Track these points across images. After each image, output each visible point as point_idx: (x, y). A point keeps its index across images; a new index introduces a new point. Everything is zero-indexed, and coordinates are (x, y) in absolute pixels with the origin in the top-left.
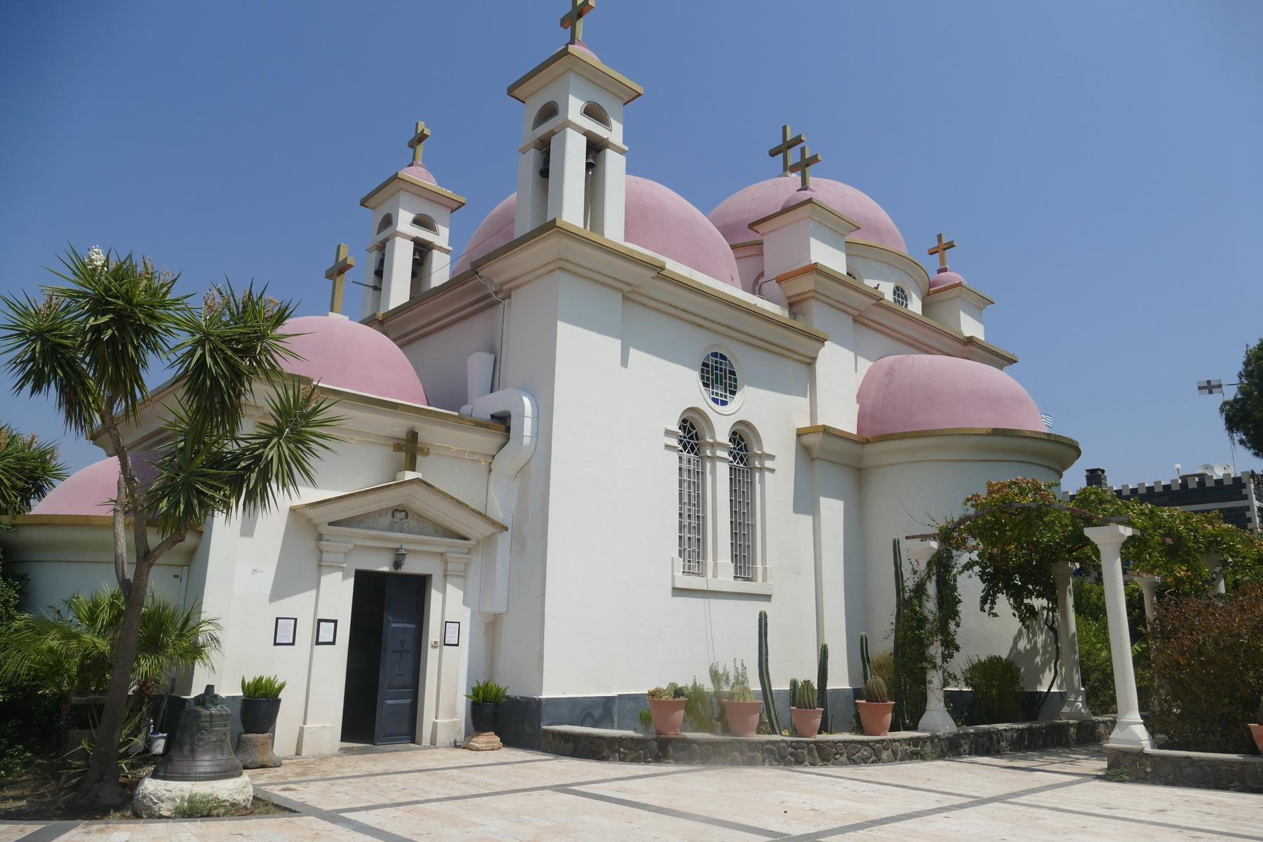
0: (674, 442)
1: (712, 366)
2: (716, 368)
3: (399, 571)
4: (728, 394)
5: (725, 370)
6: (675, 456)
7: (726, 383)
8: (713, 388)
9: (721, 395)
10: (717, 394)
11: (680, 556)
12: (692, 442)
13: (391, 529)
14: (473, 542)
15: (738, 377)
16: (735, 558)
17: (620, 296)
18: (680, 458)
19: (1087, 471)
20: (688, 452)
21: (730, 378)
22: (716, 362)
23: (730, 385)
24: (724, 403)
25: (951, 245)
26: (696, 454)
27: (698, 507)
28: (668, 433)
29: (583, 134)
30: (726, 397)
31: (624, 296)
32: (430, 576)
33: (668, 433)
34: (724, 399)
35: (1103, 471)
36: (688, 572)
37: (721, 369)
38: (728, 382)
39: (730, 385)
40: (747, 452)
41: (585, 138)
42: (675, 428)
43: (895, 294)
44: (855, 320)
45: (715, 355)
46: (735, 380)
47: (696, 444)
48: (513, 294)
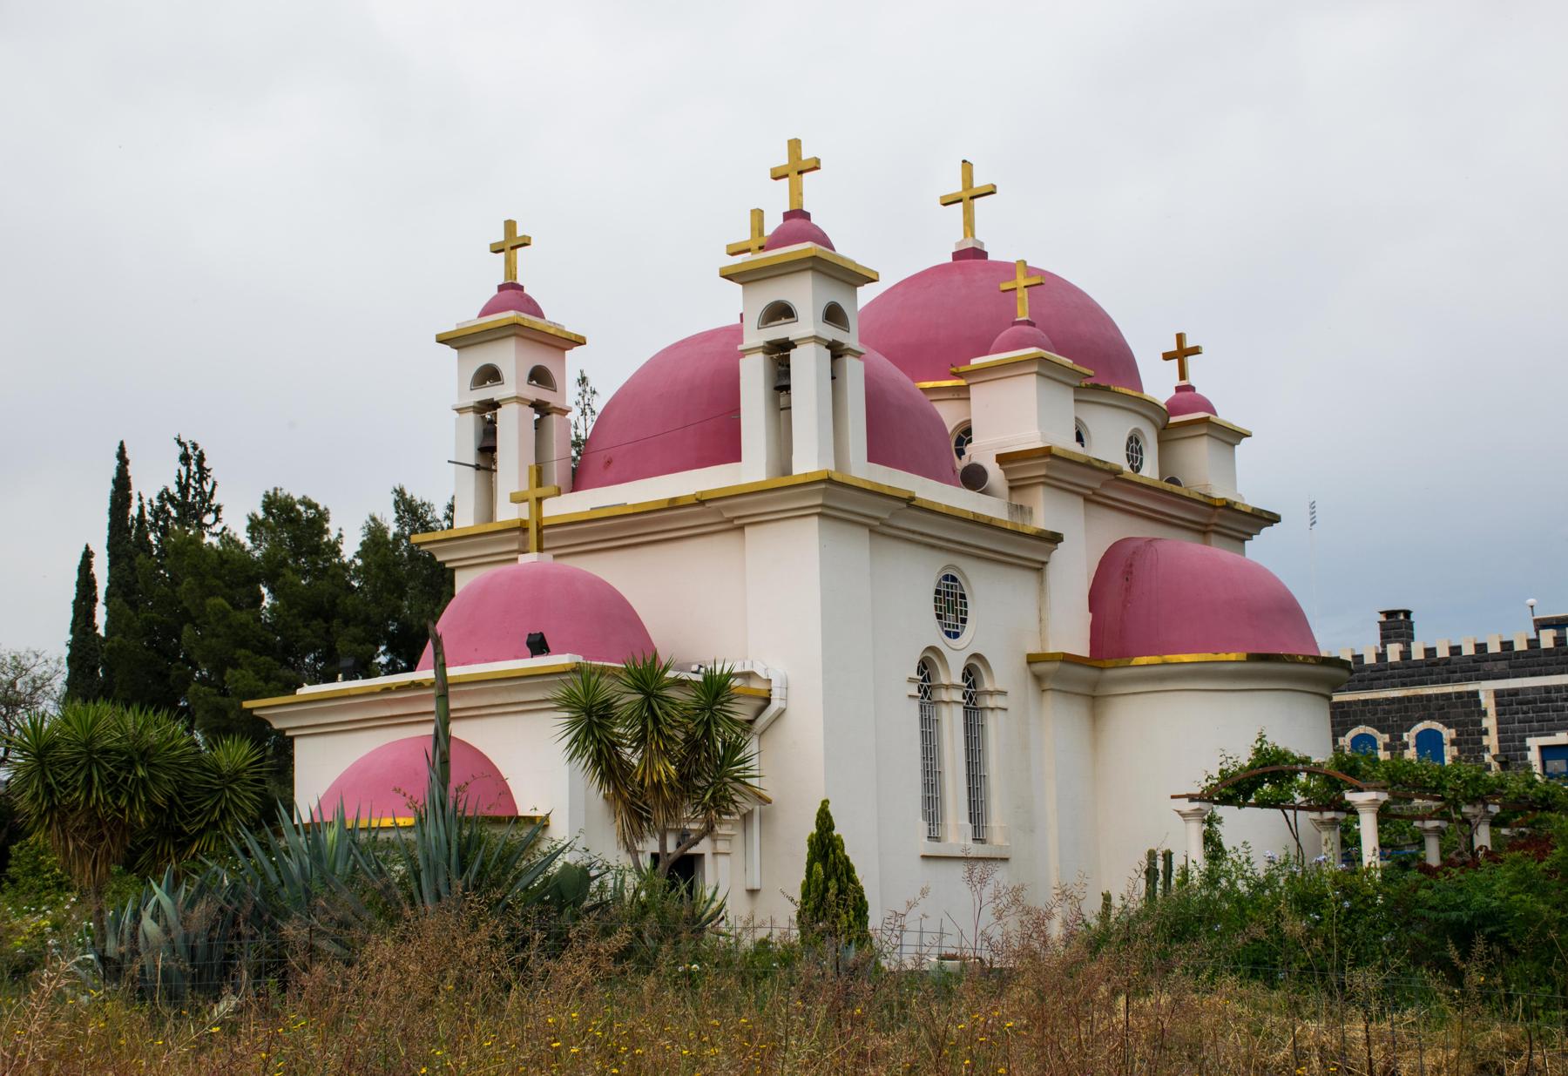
4: (960, 624)
6: (916, 704)
15: (969, 600)
17: (867, 531)
19: (1381, 613)
23: (961, 610)
24: (956, 635)
25: (1196, 351)
26: (929, 699)
28: (911, 680)
29: (827, 347)
31: (870, 531)
32: (703, 855)
33: (911, 680)
35: (1407, 614)
36: (933, 838)
39: (961, 610)
41: (829, 352)
42: (915, 675)
43: (1127, 450)
44: (1087, 500)
47: (929, 687)
48: (747, 530)
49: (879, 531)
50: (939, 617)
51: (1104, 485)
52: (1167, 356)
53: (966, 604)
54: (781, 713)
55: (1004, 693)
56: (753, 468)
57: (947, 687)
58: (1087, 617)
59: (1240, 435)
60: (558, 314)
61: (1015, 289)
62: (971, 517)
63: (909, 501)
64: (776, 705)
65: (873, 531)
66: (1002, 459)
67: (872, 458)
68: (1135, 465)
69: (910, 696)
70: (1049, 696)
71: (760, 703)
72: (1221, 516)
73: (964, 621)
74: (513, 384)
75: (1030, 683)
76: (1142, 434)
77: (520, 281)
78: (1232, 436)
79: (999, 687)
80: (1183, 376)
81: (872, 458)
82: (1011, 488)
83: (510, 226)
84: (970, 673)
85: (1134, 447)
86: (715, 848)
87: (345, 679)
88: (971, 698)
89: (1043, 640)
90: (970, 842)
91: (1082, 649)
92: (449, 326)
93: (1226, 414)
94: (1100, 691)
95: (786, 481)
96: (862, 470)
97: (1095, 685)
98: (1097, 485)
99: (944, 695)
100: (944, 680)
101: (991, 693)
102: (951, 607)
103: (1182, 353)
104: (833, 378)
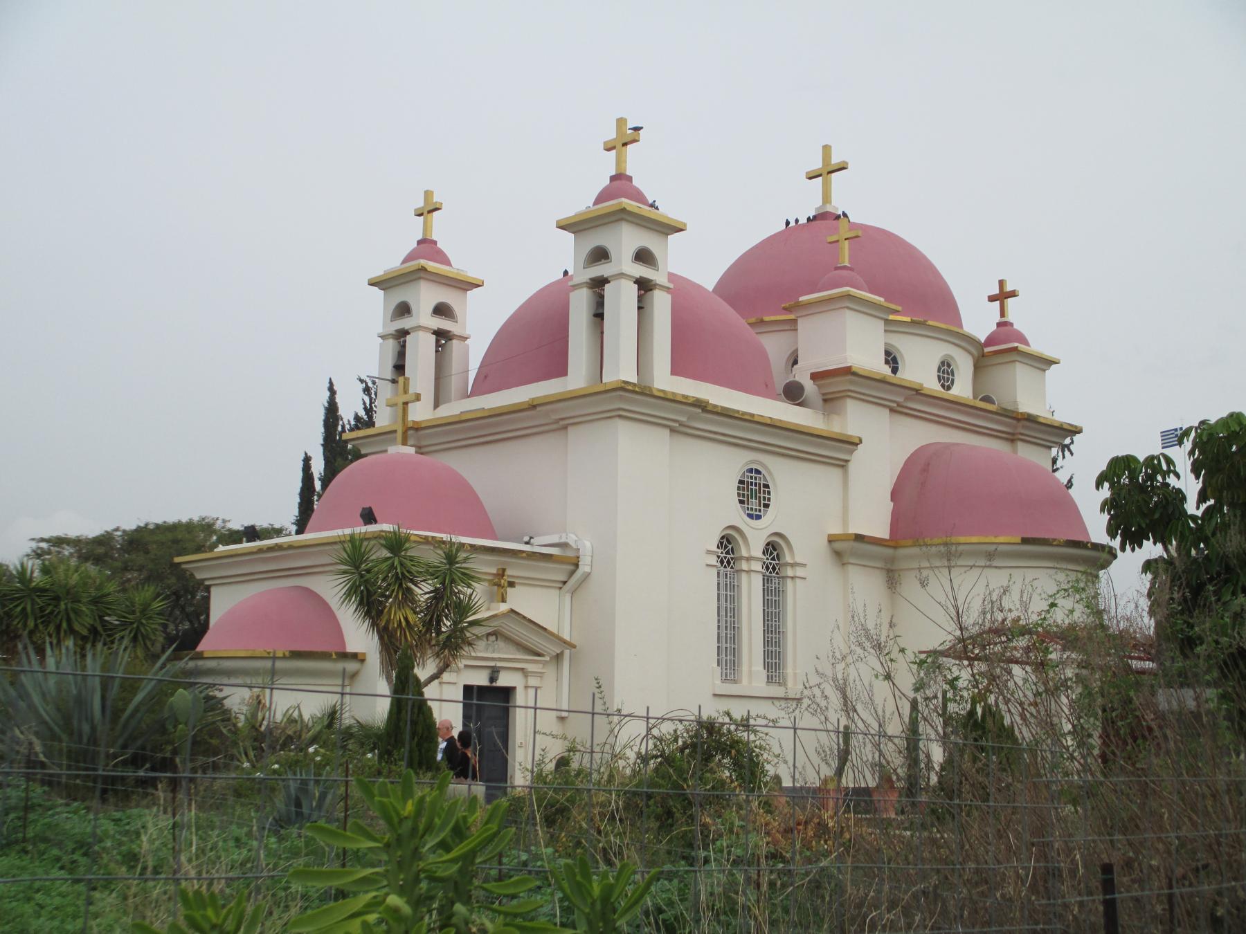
0: (713, 560)
1: (748, 482)
2: (752, 483)
3: (494, 684)
4: (762, 508)
5: (760, 484)
6: (715, 571)
7: (760, 497)
8: (748, 504)
9: (756, 510)
10: (752, 509)
11: (718, 665)
12: (728, 556)
13: (486, 650)
14: (547, 658)
15: (772, 489)
16: (767, 666)
18: (718, 573)
20: (725, 567)
21: (764, 492)
22: (751, 478)
23: (764, 498)
24: (759, 517)
25: (1013, 294)
27: (734, 617)
28: (709, 552)
30: (760, 511)
32: (514, 688)
34: (758, 513)
36: (725, 679)
37: (756, 484)
38: (762, 495)
39: (764, 498)
41: (636, 286)
42: (714, 548)
43: (939, 371)
44: (892, 410)
45: (751, 470)
46: (769, 493)
47: (732, 559)
49: (677, 430)
50: (741, 502)
51: (907, 399)
52: (992, 299)
54: (587, 576)
55: (804, 565)
56: (577, 378)
57: (748, 559)
58: (891, 505)
59: (1051, 362)
60: (462, 263)
61: (838, 241)
62: (769, 422)
63: (701, 405)
64: (584, 568)
65: (673, 430)
66: (815, 377)
67: (675, 371)
68: (946, 384)
69: (707, 565)
71: (572, 568)
72: (1024, 427)
73: (767, 506)
74: (423, 316)
76: (952, 358)
77: (434, 238)
78: (1045, 363)
79: (798, 559)
80: (1003, 314)
81: (675, 371)
82: (825, 401)
83: (428, 194)
84: (772, 548)
85: (946, 372)
86: (527, 681)
87: (248, 541)
88: (774, 568)
89: (845, 522)
90: (718, 682)
91: (883, 532)
92: (378, 272)
93: (1037, 346)
95: (602, 388)
96: (664, 379)
97: (892, 560)
98: (900, 399)
99: (744, 566)
100: (744, 553)
101: (793, 565)
102: (754, 495)
103: (1003, 296)
104: (639, 308)
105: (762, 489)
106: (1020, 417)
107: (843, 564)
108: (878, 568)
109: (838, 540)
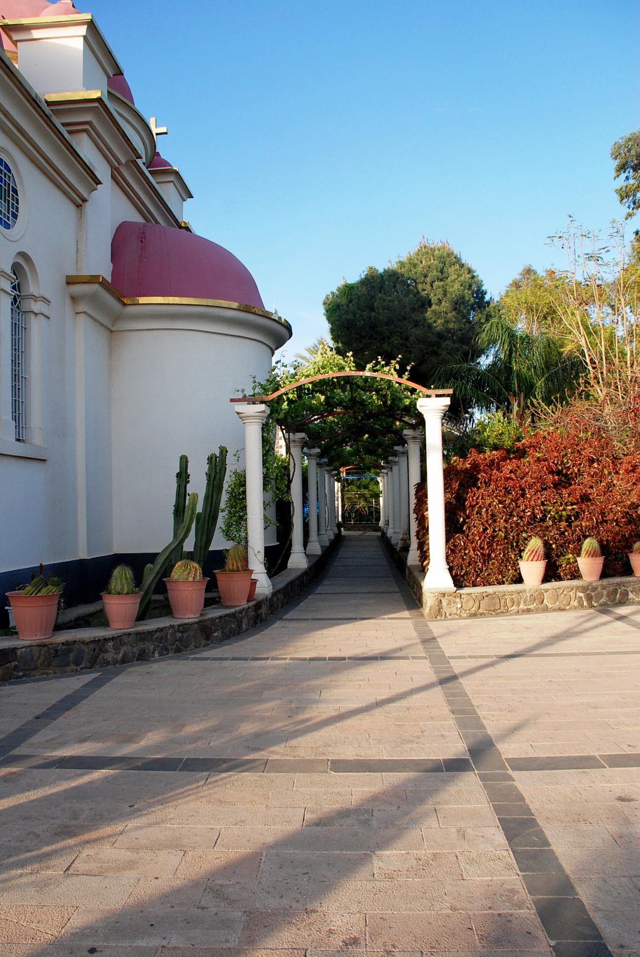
4: (11, 217)
7: (9, 201)
34: (6, 220)
40: (20, 293)
53: (17, 200)
55: (47, 301)
70: (82, 317)
73: (15, 216)
75: (68, 301)
94: (119, 326)
101: (35, 298)
105: (11, 192)
106: (183, 225)
107: (77, 313)
108: (102, 325)
109: (78, 283)
